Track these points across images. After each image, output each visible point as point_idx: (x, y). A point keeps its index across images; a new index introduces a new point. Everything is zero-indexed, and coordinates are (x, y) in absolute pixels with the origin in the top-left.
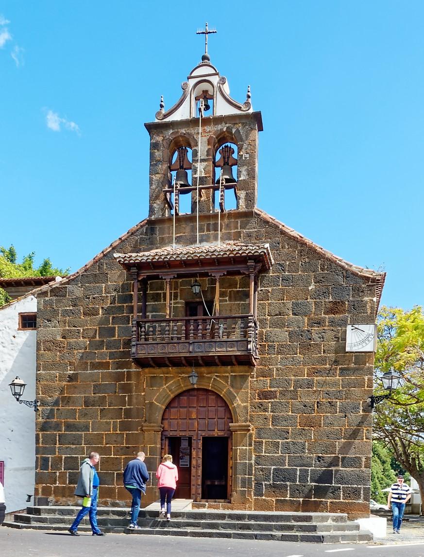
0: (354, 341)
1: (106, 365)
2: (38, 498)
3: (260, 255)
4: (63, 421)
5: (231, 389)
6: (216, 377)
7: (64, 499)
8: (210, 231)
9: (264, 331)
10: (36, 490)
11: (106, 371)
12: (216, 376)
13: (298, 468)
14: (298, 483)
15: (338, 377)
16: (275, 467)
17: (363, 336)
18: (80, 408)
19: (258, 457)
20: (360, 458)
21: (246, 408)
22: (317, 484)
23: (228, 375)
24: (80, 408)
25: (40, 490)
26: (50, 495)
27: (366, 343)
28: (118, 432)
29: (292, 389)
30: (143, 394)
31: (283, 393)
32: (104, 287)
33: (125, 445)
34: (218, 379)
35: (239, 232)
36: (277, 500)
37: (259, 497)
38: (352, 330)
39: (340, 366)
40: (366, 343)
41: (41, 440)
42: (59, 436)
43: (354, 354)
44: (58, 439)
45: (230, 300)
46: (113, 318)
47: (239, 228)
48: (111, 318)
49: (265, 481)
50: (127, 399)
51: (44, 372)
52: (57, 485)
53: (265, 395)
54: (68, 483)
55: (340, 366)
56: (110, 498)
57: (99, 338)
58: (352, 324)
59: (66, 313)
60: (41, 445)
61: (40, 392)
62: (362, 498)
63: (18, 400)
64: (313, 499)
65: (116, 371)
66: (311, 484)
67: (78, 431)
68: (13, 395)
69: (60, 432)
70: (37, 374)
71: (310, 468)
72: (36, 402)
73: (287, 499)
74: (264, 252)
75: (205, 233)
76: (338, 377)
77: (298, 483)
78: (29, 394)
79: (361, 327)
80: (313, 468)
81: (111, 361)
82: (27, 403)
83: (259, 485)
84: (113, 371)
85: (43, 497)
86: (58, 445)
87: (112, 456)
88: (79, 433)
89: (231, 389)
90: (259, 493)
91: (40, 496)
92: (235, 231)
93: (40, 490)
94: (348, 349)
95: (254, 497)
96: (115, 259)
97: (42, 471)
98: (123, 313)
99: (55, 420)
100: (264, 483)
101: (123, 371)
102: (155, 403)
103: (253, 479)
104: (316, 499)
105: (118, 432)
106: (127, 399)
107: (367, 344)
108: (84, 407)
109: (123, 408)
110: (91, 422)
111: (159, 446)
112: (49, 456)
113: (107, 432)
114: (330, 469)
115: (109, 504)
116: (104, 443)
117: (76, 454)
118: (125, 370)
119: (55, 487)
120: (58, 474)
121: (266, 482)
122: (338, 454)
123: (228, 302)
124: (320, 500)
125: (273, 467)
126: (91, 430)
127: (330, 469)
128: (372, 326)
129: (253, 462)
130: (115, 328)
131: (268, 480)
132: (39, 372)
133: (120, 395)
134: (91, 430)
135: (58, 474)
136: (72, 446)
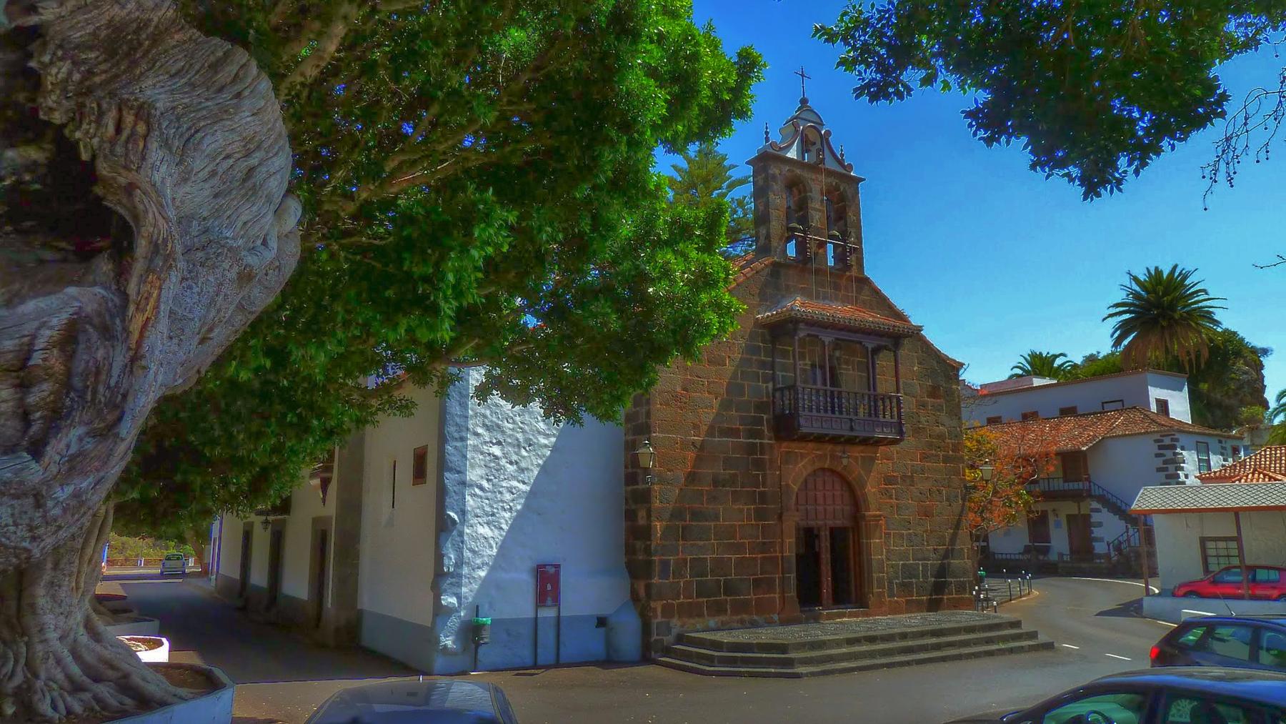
2: (658, 623)
7: (692, 621)
26: (673, 616)
28: (753, 522)
52: (681, 600)
69: (683, 523)
105: (753, 522)
118: (757, 441)
123: (851, 372)
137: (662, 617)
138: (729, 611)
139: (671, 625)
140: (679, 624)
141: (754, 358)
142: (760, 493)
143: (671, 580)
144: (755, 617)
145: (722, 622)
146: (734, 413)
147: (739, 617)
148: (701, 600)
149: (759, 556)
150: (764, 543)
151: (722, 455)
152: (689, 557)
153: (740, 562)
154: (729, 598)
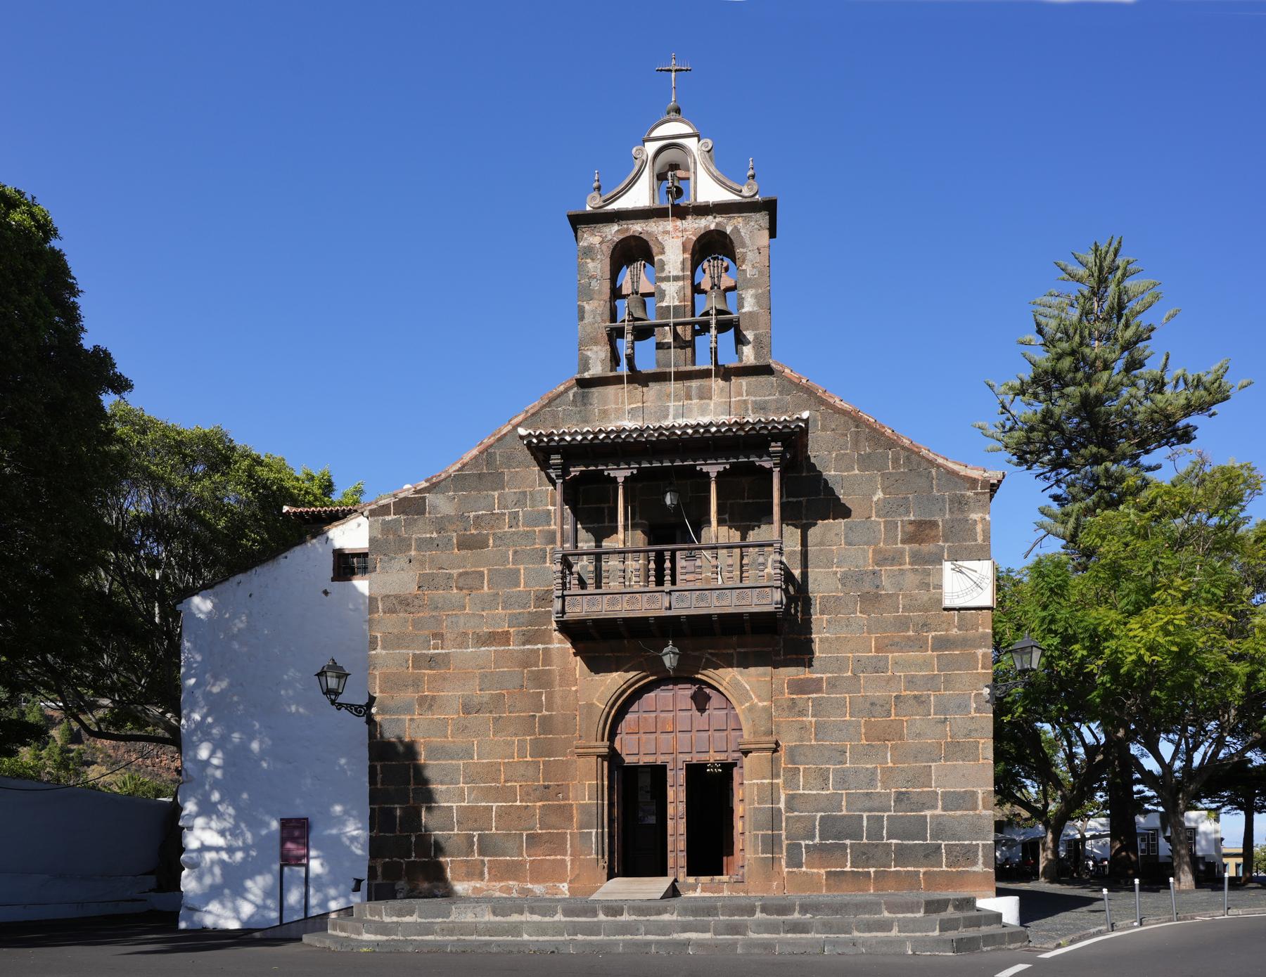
1: (504, 638)
2: (376, 885)
8: (691, 399)
10: (372, 871)
11: (503, 648)
12: (711, 654)
13: (865, 815)
15: (930, 652)
16: (823, 814)
18: (455, 717)
19: (791, 799)
20: (974, 794)
21: (765, 709)
22: (900, 842)
23: (732, 651)
24: (455, 717)
26: (400, 879)
28: (529, 759)
29: (849, 674)
30: (574, 689)
31: (833, 684)
32: (496, 497)
33: (541, 783)
36: (828, 873)
37: (795, 869)
39: (933, 634)
41: (379, 777)
44: (412, 774)
46: (515, 552)
47: (745, 394)
48: (511, 553)
49: (804, 839)
50: (543, 698)
51: (384, 652)
52: (413, 859)
55: (933, 634)
56: (515, 879)
57: (489, 588)
58: (954, 558)
59: (423, 544)
60: (379, 786)
63: (333, 702)
64: (893, 869)
65: (522, 647)
66: (889, 842)
67: (452, 759)
68: (324, 694)
71: (886, 814)
73: (845, 869)
76: (930, 652)
80: (892, 813)
81: (512, 630)
83: (794, 850)
85: (385, 882)
86: (412, 787)
87: (518, 803)
88: (453, 762)
90: (794, 861)
91: (379, 880)
95: (786, 870)
97: (382, 834)
98: (534, 544)
100: (803, 843)
101: (536, 647)
103: (784, 837)
104: (898, 869)
105: (529, 759)
106: (543, 698)
108: (461, 714)
109: (538, 715)
110: (476, 742)
113: (506, 760)
114: (923, 813)
115: (514, 891)
116: (502, 781)
117: (448, 802)
118: (540, 646)
119: (408, 863)
120: (413, 839)
121: (807, 842)
122: (936, 787)
124: (905, 869)
125: (819, 815)
126: (476, 757)
127: (923, 813)
129: (782, 805)
130: (519, 570)
131: (812, 837)
133: (532, 691)
134: (476, 757)
135: (413, 839)
137: (384, 878)
138: (486, 875)
139: (396, 888)
142: (543, 718)
143: (398, 833)
147: (502, 884)
150: (547, 787)
151: (478, 672)
153: (503, 813)
154: (486, 859)
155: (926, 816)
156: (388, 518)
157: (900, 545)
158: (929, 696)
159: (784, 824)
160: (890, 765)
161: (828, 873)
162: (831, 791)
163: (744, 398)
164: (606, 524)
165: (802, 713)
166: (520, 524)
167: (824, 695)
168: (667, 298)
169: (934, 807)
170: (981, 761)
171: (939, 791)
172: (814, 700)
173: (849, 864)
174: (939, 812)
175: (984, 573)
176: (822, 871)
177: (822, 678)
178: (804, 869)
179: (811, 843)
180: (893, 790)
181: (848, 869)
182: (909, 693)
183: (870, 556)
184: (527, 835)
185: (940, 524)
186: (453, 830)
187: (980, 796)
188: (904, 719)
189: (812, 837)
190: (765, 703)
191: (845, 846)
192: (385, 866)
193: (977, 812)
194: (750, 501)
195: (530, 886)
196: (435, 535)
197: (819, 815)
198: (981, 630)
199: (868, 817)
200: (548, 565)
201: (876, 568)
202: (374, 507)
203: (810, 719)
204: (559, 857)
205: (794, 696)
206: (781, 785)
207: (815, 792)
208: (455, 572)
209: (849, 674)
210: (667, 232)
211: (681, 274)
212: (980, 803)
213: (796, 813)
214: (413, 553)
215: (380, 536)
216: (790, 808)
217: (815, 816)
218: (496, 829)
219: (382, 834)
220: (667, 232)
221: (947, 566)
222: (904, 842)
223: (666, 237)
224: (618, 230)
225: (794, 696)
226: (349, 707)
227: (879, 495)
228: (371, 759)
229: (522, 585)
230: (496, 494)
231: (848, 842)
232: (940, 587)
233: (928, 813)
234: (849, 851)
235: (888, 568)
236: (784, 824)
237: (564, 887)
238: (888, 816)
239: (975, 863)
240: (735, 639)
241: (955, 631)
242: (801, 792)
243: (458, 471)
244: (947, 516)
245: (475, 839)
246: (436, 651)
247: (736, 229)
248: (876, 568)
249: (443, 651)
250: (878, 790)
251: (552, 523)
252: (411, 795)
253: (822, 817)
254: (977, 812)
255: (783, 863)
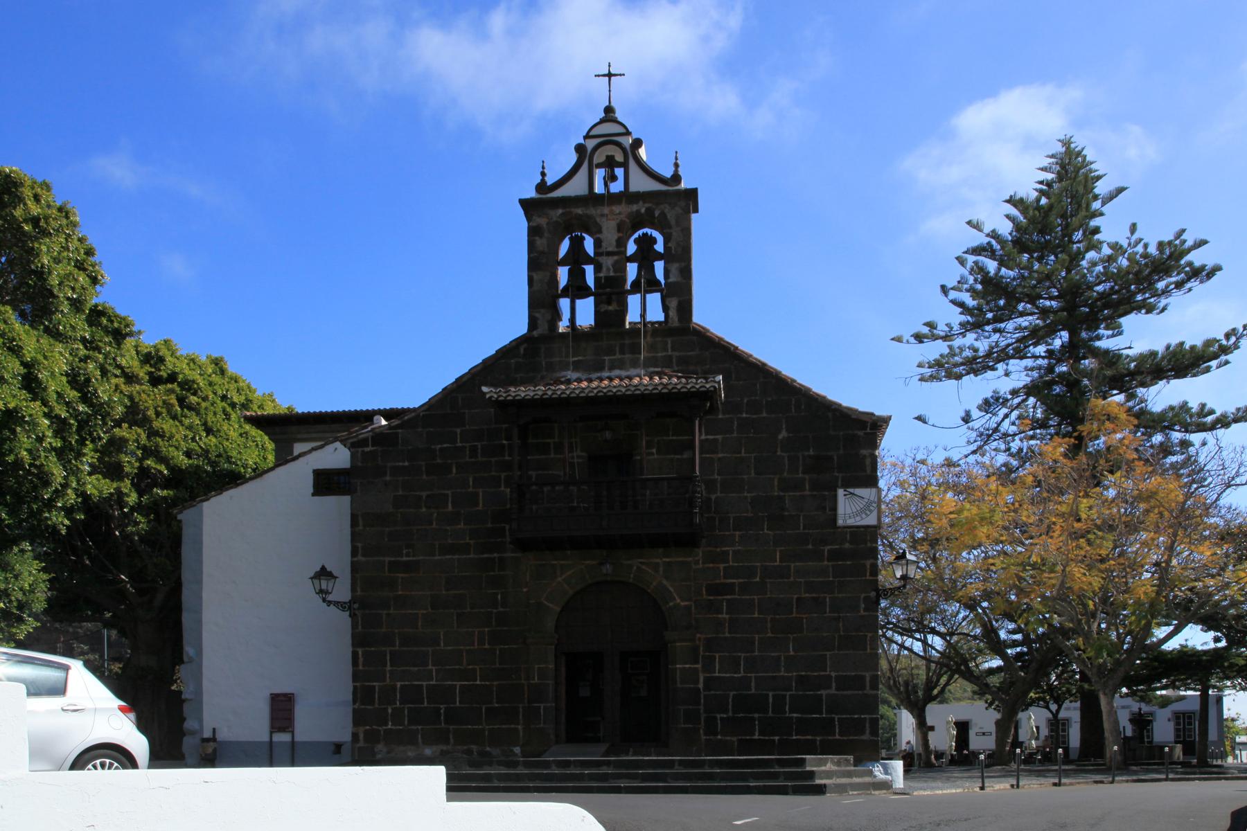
0: (849, 511)
3: (708, 391)
4: (396, 631)
5: (665, 582)
6: (640, 565)
9: (713, 497)
10: (355, 736)
12: (641, 563)
14: (770, 714)
15: (826, 563)
16: (735, 693)
17: (860, 504)
19: (707, 680)
20: (863, 678)
21: (688, 608)
22: (799, 715)
23: (658, 560)
25: (361, 736)
27: (866, 514)
28: (487, 646)
30: (525, 590)
34: (644, 567)
35: (670, 357)
36: (740, 741)
37: (711, 737)
38: (845, 495)
40: (866, 514)
41: (361, 660)
42: (390, 653)
43: (848, 530)
45: (659, 452)
48: (471, 480)
51: (363, 559)
52: (389, 727)
53: (715, 590)
54: (406, 722)
55: (829, 547)
58: (846, 485)
60: (361, 668)
61: (359, 589)
62: (868, 732)
63: (324, 600)
64: (794, 737)
68: (317, 593)
70: (352, 563)
71: (788, 693)
72: (353, 601)
74: (715, 387)
75: (618, 356)
77: (770, 714)
78: (342, 590)
79: (858, 491)
80: (794, 692)
81: (472, 542)
82: (340, 605)
84: (476, 556)
86: (388, 668)
87: (478, 682)
89: (665, 582)
92: (664, 354)
93: (361, 736)
94: (840, 522)
96: (485, 394)
97: (363, 707)
99: (383, 630)
100: (718, 716)
102: (546, 603)
103: (702, 711)
104: (798, 737)
105: (487, 646)
107: (867, 515)
108: (430, 610)
109: (495, 611)
110: (442, 633)
111: (552, 666)
112: (374, 684)
113: (468, 648)
118: (495, 555)
119: (385, 730)
120: (390, 711)
121: (722, 715)
123: (656, 456)
125: (732, 694)
126: (442, 645)
128: (874, 490)
129: (701, 686)
131: (726, 711)
132: (356, 559)
134: (442, 645)
135: (390, 711)
136: (412, 668)
138: (452, 741)
139: (376, 750)
140: (385, 750)
141: (493, 460)
144: (488, 749)
145: (442, 750)
146: (462, 526)
147: (465, 747)
148: (414, 727)
149: (495, 683)
152: (399, 684)
154: (451, 727)
155: (822, 695)
156: (367, 449)
157: (800, 475)
158: (825, 598)
159: (702, 701)
160: (792, 653)
161: (740, 741)
162: (742, 674)
163: (670, 353)
164: (552, 456)
165: (719, 611)
166: (479, 455)
167: (736, 597)
168: (604, 269)
169: (829, 687)
170: (869, 651)
171: (833, 674)
172: (728, 600)
173: (757, 734)
174: (833, 691)
175: (872, 499)
176: (735, 739)
177: (734, 583)
178: (719, 737)
179: (725, 716)
180: (795, 674)
181: (756, 737)
182: (807, 595)
183: (776, 483)
184: (486, 709)
185: (835, 458)
186: (423, 703)
187: (868, 679)
188: (804, 616)
189: (726, 711)
190: (687, 603)
191: (753, 719)
192: (366, 732)
193: (865, 692)
194: (674, 438)
195: (488, 749)
196: (406, 464)
197: (732, 694)
198: (869, 545)
199: (773, 696)
200: (502, 489)
201: (782, 494)
202: (355, 440)
203: (724, 616)
204: (513, 726)
205: (712, 598)
206: (700, 669)
207: (728, 675)
208: (424, 494)
209: (758, 579)
210: (602, 215)
211: (616, 250)
212: (868, 684)
213: (712, 692)
214: (388, 478)
215: (360, 464)
216: (707, 688)
217: (729, 695)
218: (460, 703)
219: (363, 707)
220: (602, 215)
221: (841, 492)
222: (804, 716)
223: (604, 219)
224: (563, 214)
225: (712, 598)
226: (336, 604)
227: (783, 434)
228: (353, 645)
229: (481, 505)
230: (458, 431)
231: (756, 715)
232: (834, 509)
233: (824, 692)
234: (757, 723)
235: (791, 494)
236: (702, 701)
237: (517, 750)
238: (790, 695)
239: (863, 733)
240: (661, 550)
241: (847, 545)
242: (717, 675)
243: (425, 411)
244: (841, 452)
245: (442, 711)
246: (408, 559)
247: (663, 214)
248: (782, 494)
249: (414, 559)
250: (782, 674)
251: (507, 454)
252: (388, 675)
253: (734, 695)
254: (865, 692)
255: (701, 731)
